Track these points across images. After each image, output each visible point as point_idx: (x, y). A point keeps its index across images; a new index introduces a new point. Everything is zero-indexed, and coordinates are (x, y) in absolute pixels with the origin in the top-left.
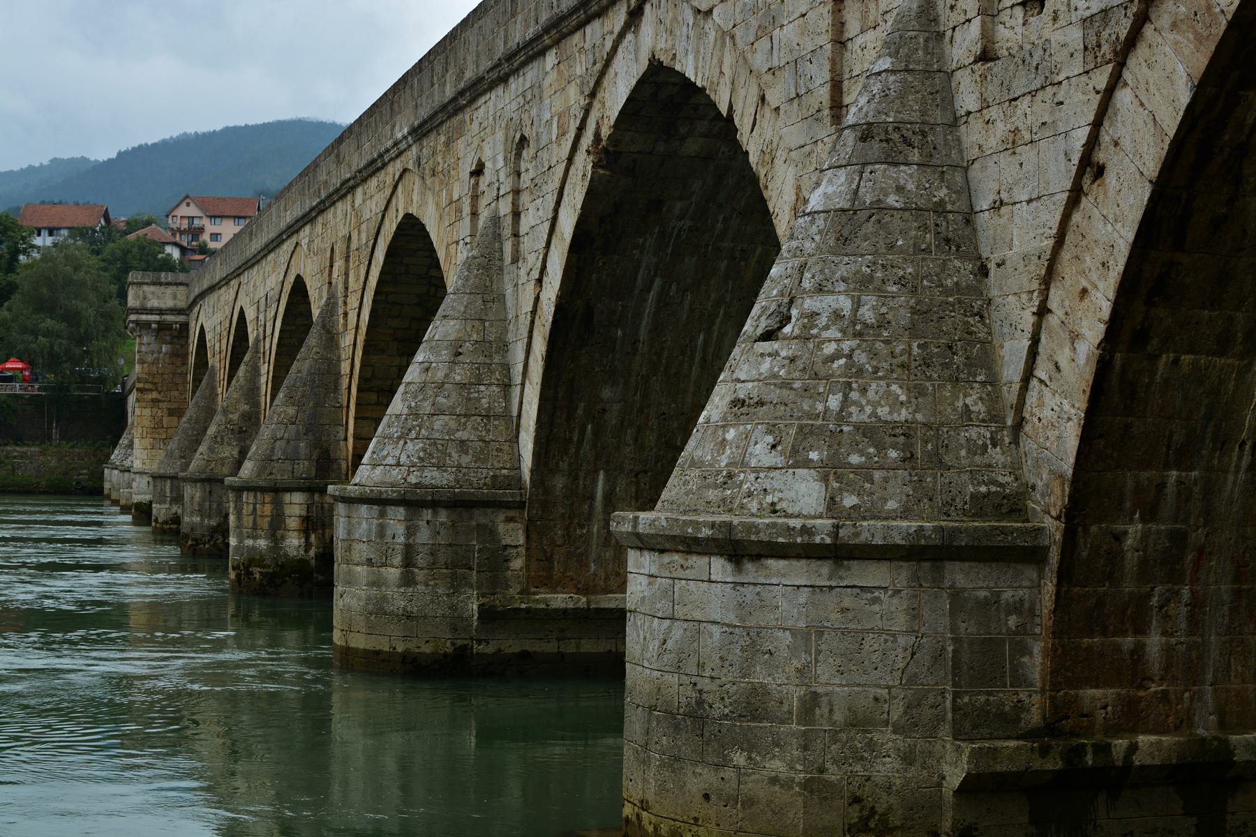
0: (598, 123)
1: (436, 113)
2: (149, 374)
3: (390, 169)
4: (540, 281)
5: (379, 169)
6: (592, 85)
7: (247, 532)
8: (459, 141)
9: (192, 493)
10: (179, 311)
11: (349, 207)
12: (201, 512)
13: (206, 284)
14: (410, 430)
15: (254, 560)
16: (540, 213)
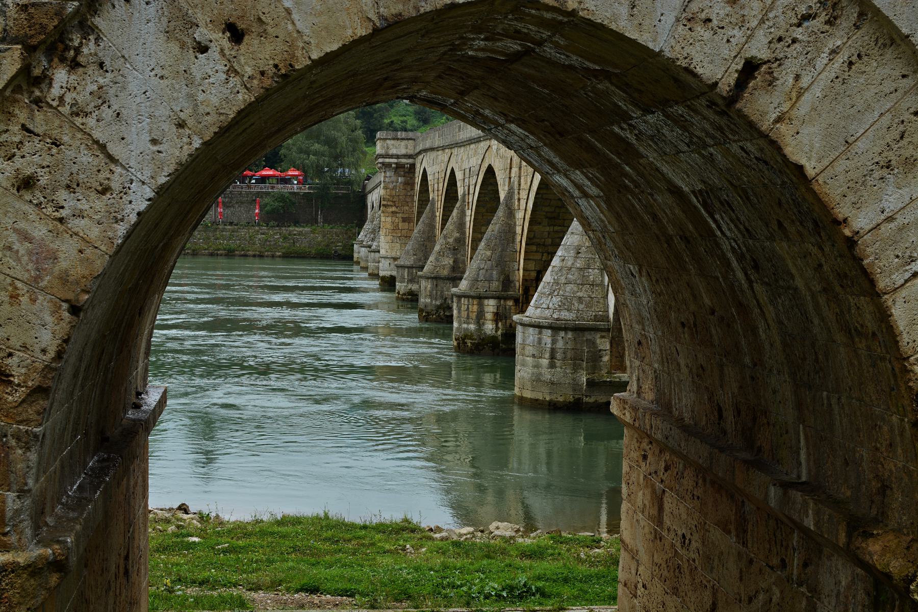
2: (390, 196)
12: (431, 296)
13: (428, 146)
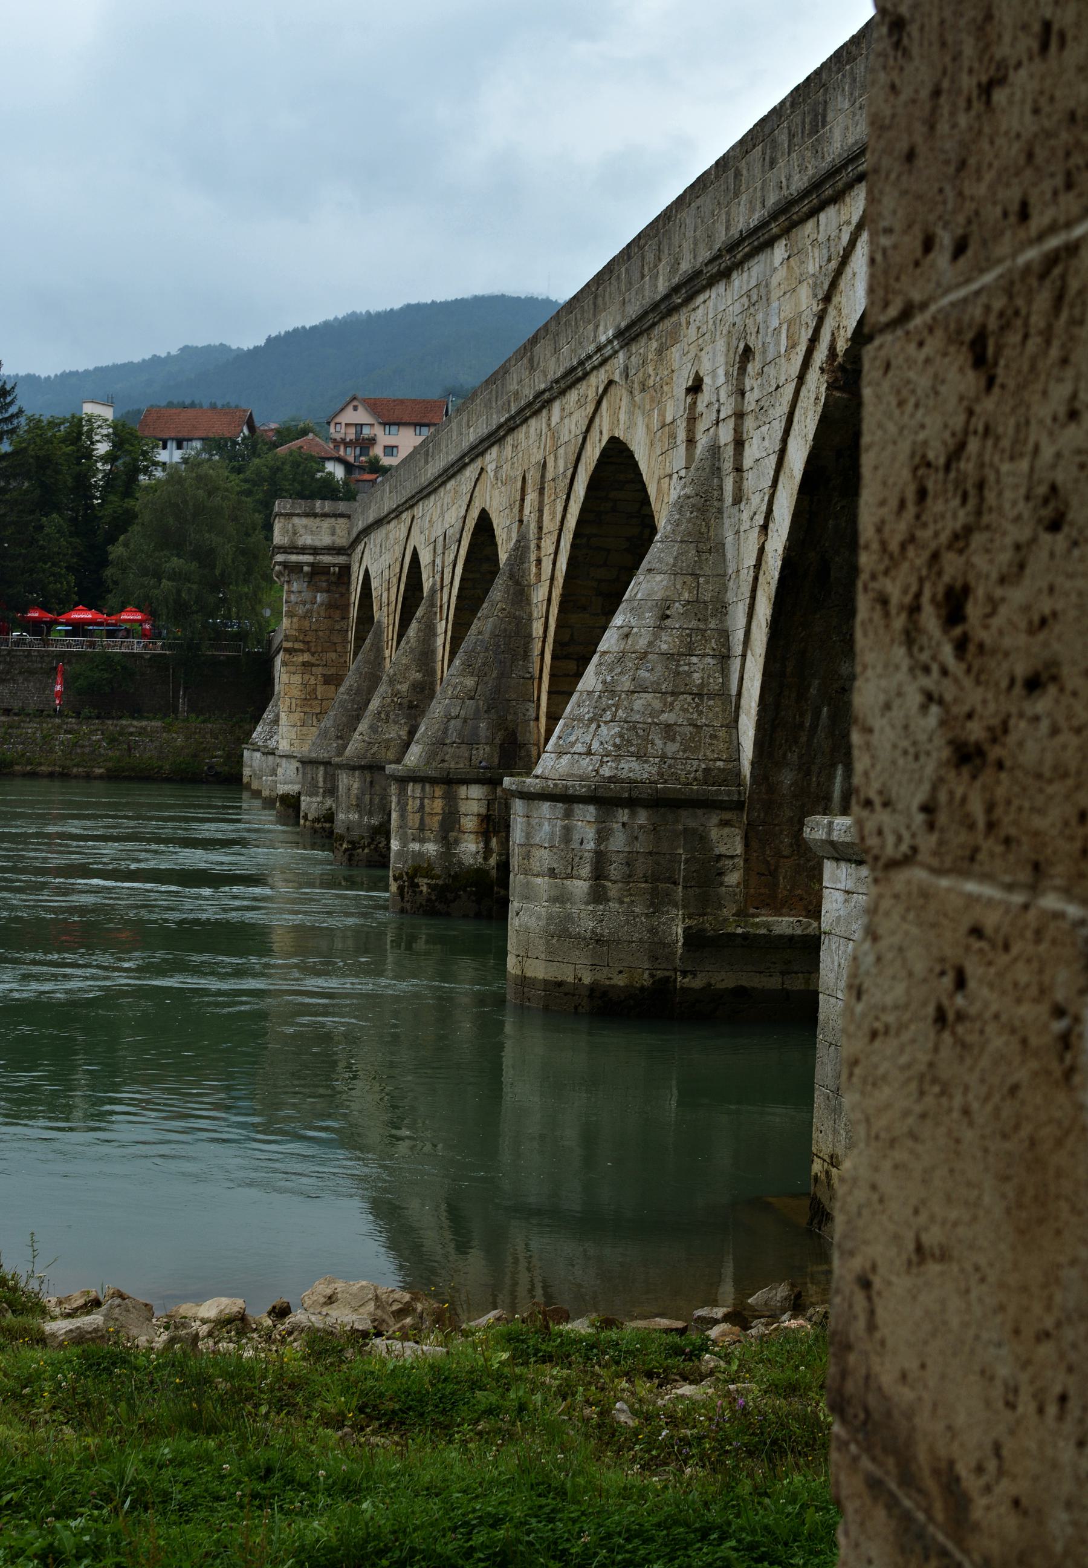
0: (833, 334)
1: (645, 314)
2: (300, 630)
3: (593, 379)
4: (765, 528)
5: (579, 380)
6: (826, 286)
7: (412, 834)
8: (674, 349)
9: (349, 783)
10: (338, 551)
11: (544, 426)
12: (359, 807)
13: (371, 518)
14: (604, 710)
15: (418, 869)
16: (766, 443)
